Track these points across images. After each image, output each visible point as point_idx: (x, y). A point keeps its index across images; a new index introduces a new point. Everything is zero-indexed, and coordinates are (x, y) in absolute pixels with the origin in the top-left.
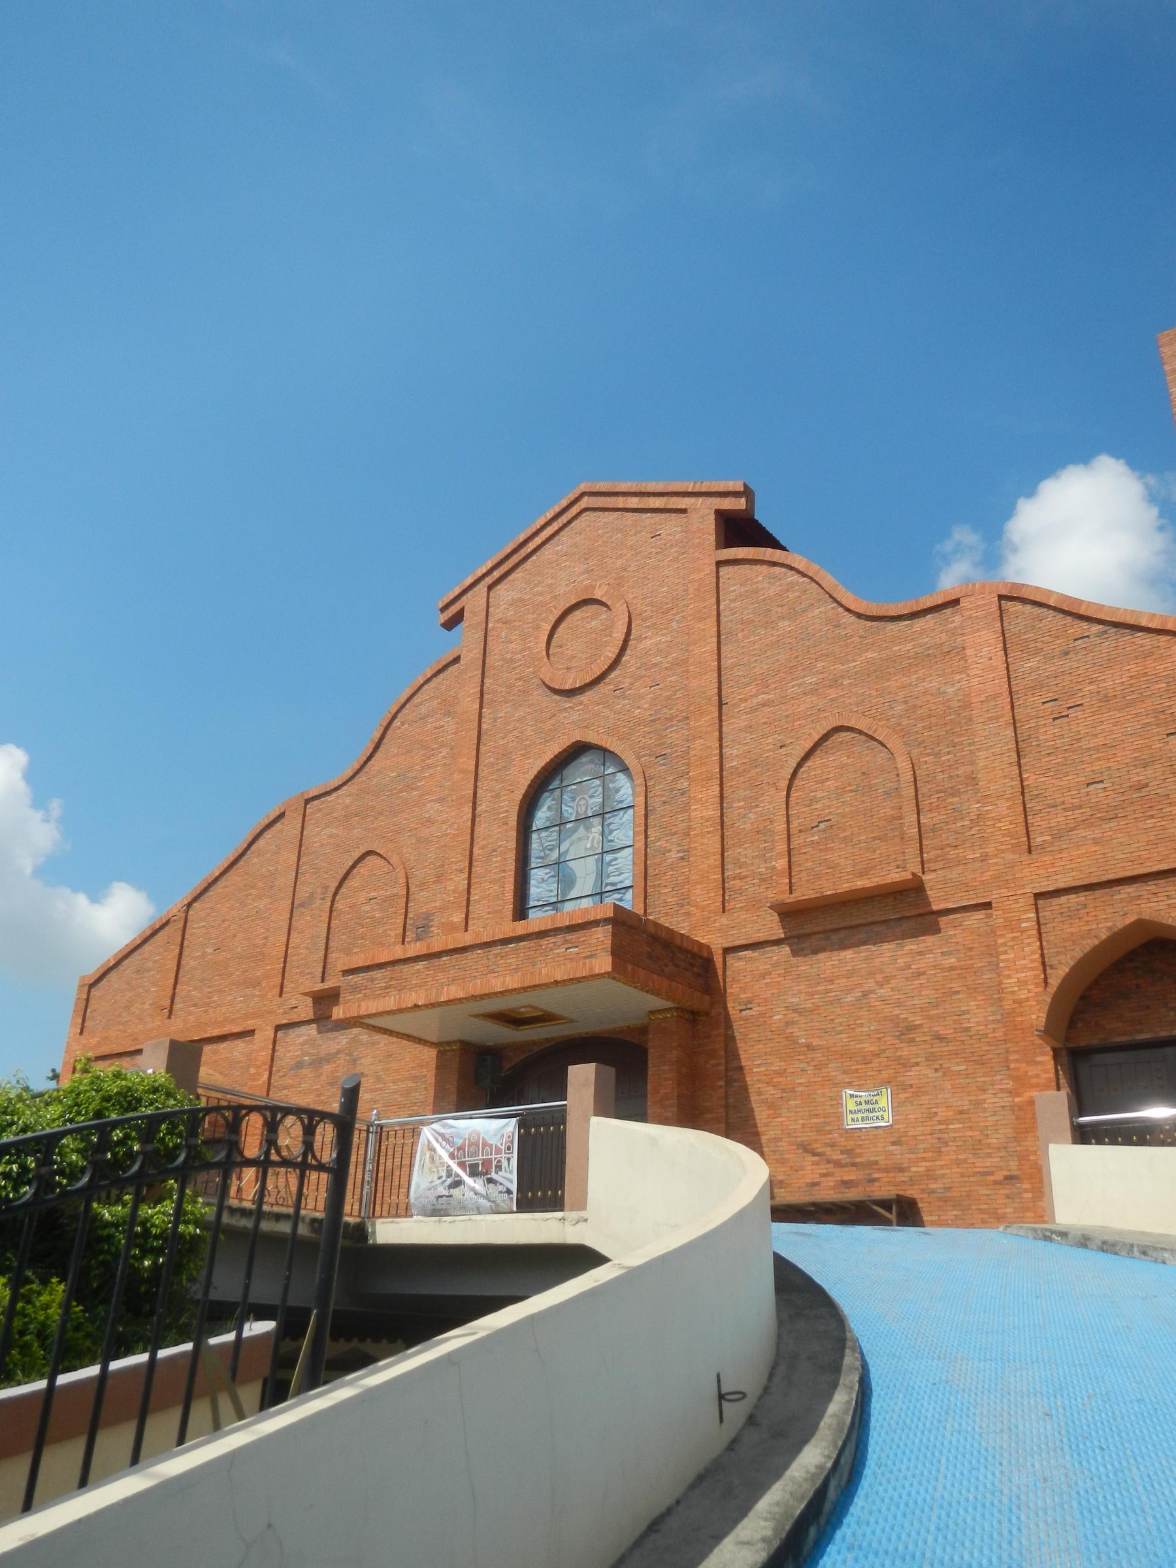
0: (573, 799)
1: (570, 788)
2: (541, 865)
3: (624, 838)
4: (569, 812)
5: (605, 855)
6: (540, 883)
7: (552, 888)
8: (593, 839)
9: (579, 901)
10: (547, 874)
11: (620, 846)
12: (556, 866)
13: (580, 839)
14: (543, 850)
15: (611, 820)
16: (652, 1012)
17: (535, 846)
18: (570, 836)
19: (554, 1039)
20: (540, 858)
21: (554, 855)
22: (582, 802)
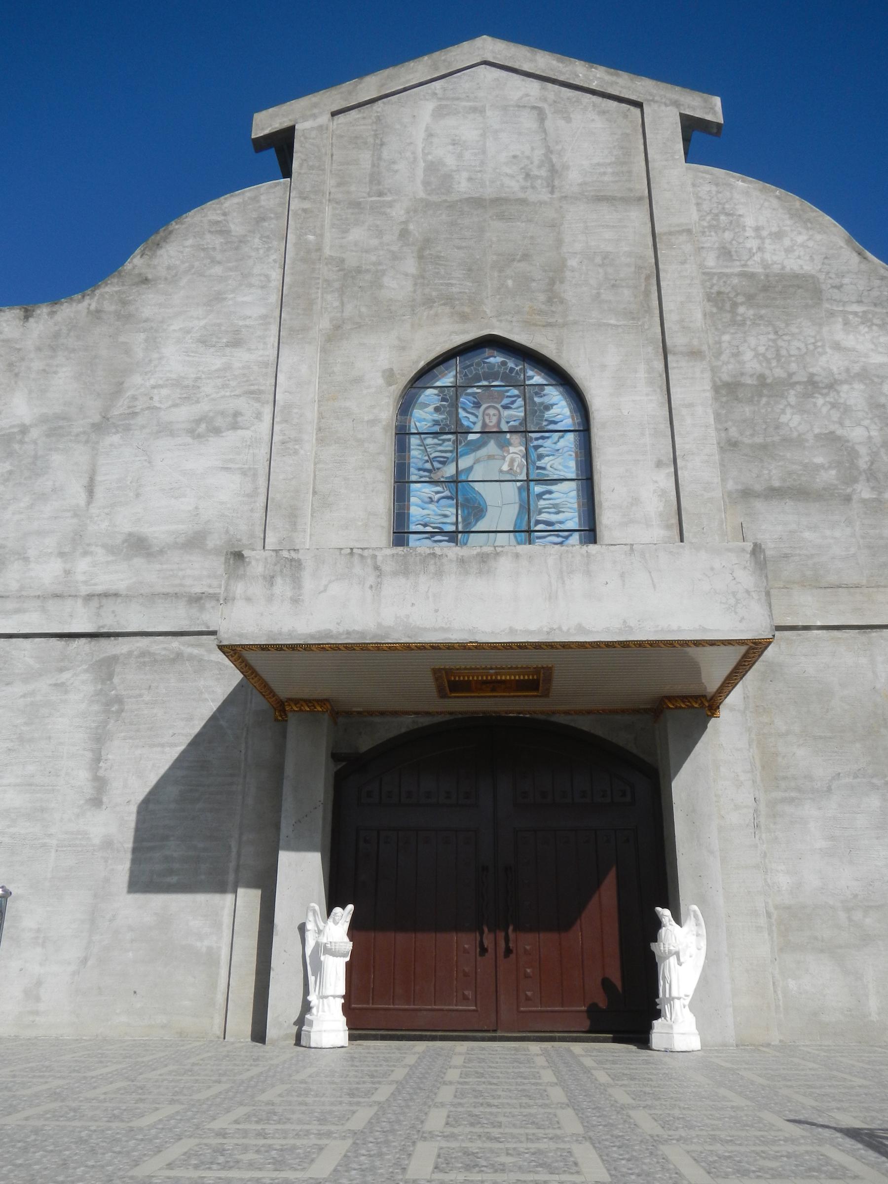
0: (477, 405)
1: (470, 390)
2: (427, 479)
5: (532, 484)
6: (426, 503)
8: (512, 461)
11: (555, 477)
13: (490, 457)
14: (430, 461)
15: (540, 442)
16: (670, 698)
17: (415, 452)
18: (474, 451)
19: (461, 713)
20: (425, 470)
21: (449, 471)
22: (492, 412)
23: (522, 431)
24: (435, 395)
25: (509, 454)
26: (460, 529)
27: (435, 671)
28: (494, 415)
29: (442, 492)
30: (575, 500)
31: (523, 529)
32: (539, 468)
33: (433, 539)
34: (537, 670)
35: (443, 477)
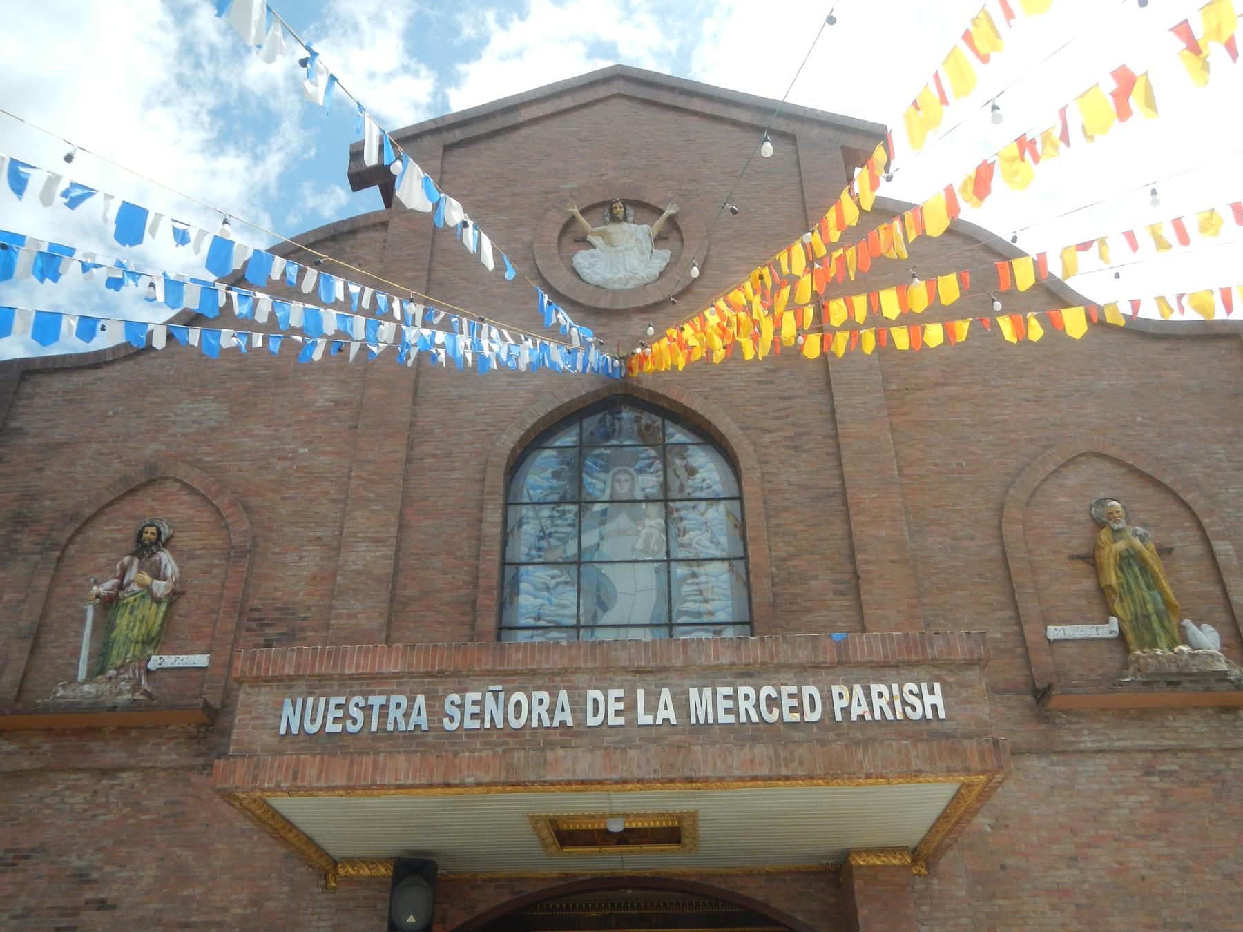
0: (606, 469)
1: (597, 451)
3: (708, 544)
4: (597, 485)
5: (673, 565)
6: (540, 590)
7: (567, 602)
9: (623, 630)
10: (553, 577)
11: (702, 556)
12: (574, 568)
13: (621, 532)
15: (683, 513)
16: (859, 851)
21: (572, 549)
22: (623, 477)
23: (664, 499)
24: (554, 457)
25: (644, 526)
26: (583, 622)
27: (534, 820)
28: (626, 481)
29: (559, 577)
30: (726, 586)
31: (663, 622)
32: (683, 546)
33: (547, 636)
34: (680, 817)
35: (561, 557)
